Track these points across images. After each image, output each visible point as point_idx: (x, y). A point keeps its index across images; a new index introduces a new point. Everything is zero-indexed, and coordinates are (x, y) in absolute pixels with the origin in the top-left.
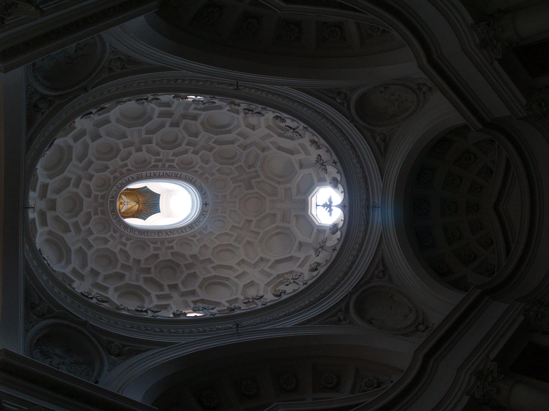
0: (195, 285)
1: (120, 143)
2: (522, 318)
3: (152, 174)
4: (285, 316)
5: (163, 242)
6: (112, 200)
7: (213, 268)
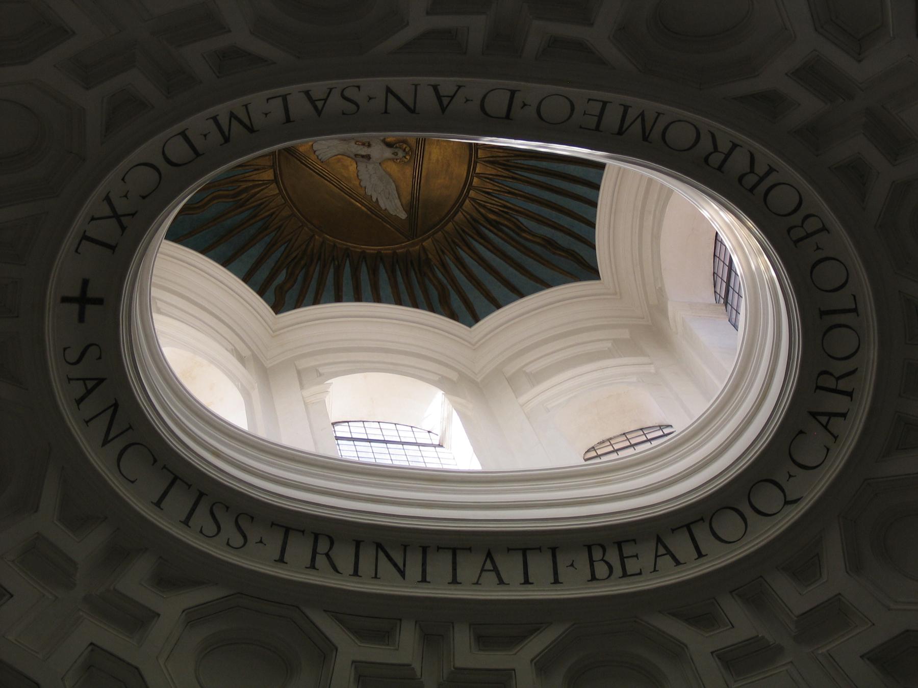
6: (836, 403)
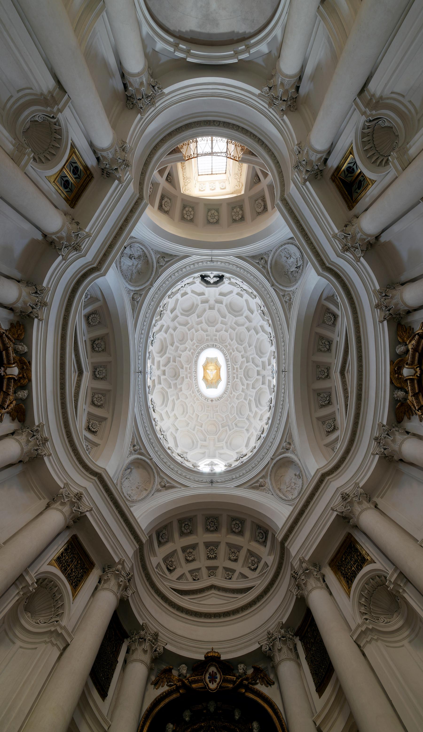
0: (163, 385)
1: (246, 344)
2: (117, 560)
3: (229, 368)
4: (142, 415)
5: (190, 373)
6: (214, 345)
7: (174, 399)
